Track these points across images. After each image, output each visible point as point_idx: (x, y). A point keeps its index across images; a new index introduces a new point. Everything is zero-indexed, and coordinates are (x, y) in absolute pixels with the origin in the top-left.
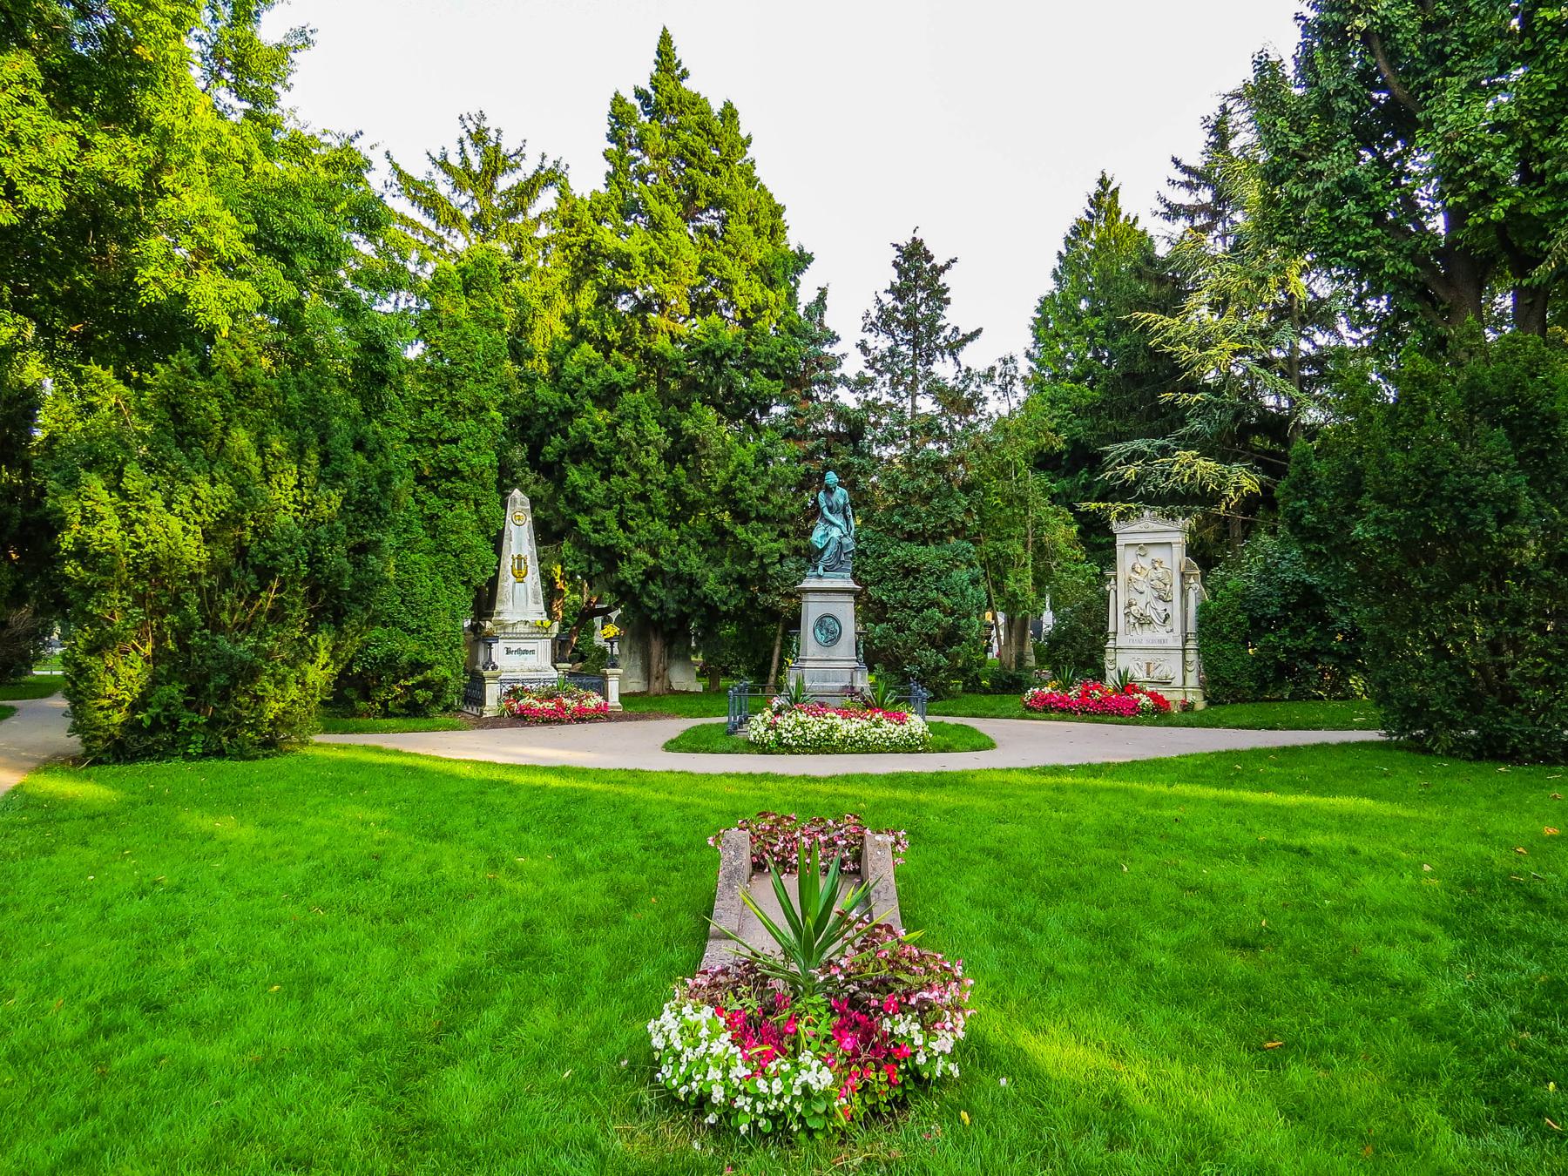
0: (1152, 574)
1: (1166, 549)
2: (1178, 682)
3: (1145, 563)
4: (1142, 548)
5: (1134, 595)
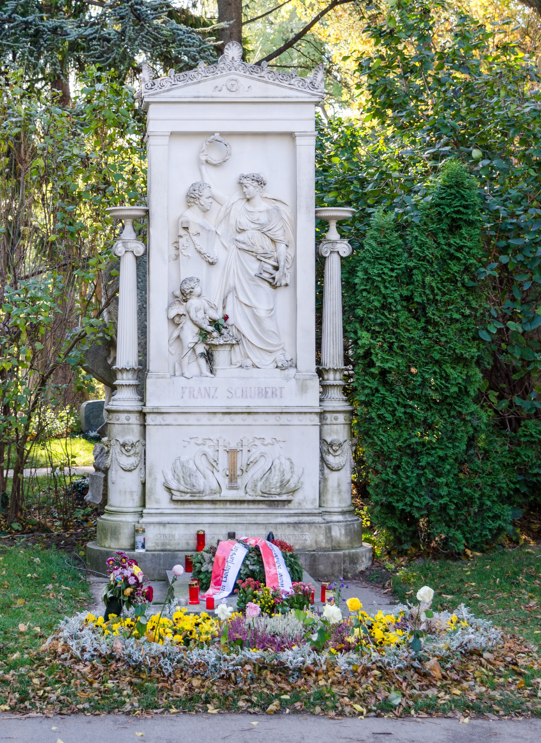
0: (240, 214)
1: (278, 149)
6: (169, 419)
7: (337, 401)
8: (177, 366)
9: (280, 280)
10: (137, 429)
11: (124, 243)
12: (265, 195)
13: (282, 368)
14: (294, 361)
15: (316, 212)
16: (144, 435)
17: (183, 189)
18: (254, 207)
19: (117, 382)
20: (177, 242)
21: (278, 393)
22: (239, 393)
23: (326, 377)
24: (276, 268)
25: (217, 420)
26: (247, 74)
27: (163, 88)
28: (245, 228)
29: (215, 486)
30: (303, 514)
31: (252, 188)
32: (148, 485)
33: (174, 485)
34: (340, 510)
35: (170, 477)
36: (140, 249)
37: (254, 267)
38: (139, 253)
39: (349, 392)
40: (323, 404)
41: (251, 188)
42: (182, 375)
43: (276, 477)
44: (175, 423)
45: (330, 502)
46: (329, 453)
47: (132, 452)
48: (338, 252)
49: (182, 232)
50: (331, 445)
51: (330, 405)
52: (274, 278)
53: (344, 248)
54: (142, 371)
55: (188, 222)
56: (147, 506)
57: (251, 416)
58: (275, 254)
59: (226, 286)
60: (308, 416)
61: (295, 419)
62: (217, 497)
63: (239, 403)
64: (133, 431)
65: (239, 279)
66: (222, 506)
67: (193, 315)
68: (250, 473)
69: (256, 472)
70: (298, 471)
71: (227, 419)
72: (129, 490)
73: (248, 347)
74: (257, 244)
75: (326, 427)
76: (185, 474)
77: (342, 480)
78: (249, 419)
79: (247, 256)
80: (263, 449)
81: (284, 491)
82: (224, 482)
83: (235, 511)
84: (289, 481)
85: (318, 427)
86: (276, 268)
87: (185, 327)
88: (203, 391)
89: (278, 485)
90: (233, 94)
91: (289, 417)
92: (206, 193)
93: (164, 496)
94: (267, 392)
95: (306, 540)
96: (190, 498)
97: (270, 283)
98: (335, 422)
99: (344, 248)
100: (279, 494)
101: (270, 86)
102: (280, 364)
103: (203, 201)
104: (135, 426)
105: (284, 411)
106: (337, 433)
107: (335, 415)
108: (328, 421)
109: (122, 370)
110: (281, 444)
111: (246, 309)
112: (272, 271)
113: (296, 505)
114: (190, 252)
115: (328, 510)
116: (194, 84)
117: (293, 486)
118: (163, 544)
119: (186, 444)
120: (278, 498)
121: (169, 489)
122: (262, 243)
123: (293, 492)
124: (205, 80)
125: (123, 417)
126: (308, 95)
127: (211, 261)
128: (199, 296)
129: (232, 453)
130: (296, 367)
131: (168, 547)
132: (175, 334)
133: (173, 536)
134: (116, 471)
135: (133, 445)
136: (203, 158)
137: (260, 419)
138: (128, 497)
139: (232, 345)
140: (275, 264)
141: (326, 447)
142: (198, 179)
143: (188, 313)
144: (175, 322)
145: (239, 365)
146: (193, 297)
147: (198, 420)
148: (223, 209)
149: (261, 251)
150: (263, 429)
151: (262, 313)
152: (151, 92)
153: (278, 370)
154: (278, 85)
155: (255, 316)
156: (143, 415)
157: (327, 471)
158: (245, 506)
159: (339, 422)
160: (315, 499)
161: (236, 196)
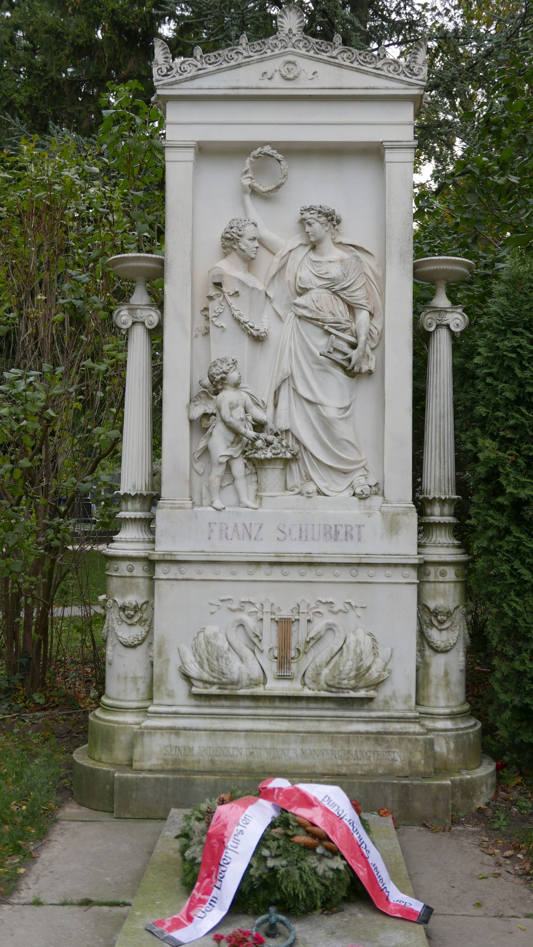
2: (402, 683)
3: (276, 226)
4: (264, 163)
5: (229, 346)
6: (190, 572)
7: (444, 548)
8: (204, 491)
9: (358, 362)
10: (143, 584)
11: (132, 310)
12: (339, 239)
13: (362, 497)
14: (380, 486)
15: (416, 267)
16: (151, 592)
17: (218, 231)
18: (322, 255)
20: (206, 309)
21: (355, 533)
22: (295, 533)
23: (429, 511)
24: (354, 346)
25: (261, 574)
26: (312, 53)
27: (185, 75)
28: (308, 286)
29: (256, 673)
31: (318, 227)
32: (156, 670)
33: (194, 670)
34: (447, 711)
36: (152, 317)
37: (319, 343)
38: (151, 323)
39: (462, 533)
40: (422, 550)
41: (317, 225)
42: (211, 504)
43: (350, 663)
44: (197, 577)
45: (433, 699)
46: (433, 625)
47: (136, 619)
48: (448, 326)
49: (213, 292)
50: (435, 613)
51: (435, 554)
52: (349, 360)
53: (457, 320)
54: (152, 499)
55: (221, 276)
56: (155, 701)
58: (354, 327)
59: (279, 372)
60: (400, 570)
61: (380, 575)
62: (259, 691)
63: (295, 549)
64: (138, 587)
65: (298, 361)
66: (267, 704)
67: (225, 413)
68: (311, 655)
69: (320, 654)
70: (384, 652)
71: (277, 573)
72: (131, 675)
73: (311, 464)
74: (325, 309)
75: (428, 586)
76: (210, 656)
77: (450, 665)
78: (311, 574)
79: (309, 327)
80: (331, 619)
81: (361, 684)
82: (271, 668)
83: (287, 712)
84: (369, 668)
85: (415, 587)
86: (354, 346)
87: (215, 432)
88: (240, 528)
89: (353, 674)
90: (290, 85)
91: (371, 571)
92: (249, 231)
93: (180, 688)
94: (337, 533)
95: (394, 760)
97: (344, 368)
98: (441, 579)
99: (457, 320)
101: (345, 72)
102: (358, 491)
103: (245, 244)
104: (141, 581)
105: (363, 561)
106: (444, 595)
107: (442, 568)
108: (431, 578)
109: (127, 497)
110: (359, 612)
111: (308, 407)
112: (345, 348)
113: (381, 704)
114: (225, 321)
115: (430, 710)
117: (375, 675)
119: (213, 609)
120: (352, 694)
121: (187, 678)
123: (377, 685)
124: (248, 64)
125: (123, 566)
126: (403, 86)
127: (255, 333)
128: (236, 386)
130: (383, 495)
131: (182, 766)
132: (202, 445)
133: (191, 749)
134: (114, 646)
135: (136, 609)
136: (247, 182)
137: (328, 574)
138: (130, 685)
139: (287, 462)
140: (352, 339)
142: (239, 214)
143: (219, 410)
144: (200, 425)
145: (297, 490)
146: (228, 387)
147: (233, 574)
148: (276, 260)
149: (330, 318)
151: (331, 413)
152: (167, 80)
153: (355, 499)
154: (358, 70)
157: (428, 652)
158: (304, 704)
159: (447, 579)
160: (410, 696)
161: (296, 240)
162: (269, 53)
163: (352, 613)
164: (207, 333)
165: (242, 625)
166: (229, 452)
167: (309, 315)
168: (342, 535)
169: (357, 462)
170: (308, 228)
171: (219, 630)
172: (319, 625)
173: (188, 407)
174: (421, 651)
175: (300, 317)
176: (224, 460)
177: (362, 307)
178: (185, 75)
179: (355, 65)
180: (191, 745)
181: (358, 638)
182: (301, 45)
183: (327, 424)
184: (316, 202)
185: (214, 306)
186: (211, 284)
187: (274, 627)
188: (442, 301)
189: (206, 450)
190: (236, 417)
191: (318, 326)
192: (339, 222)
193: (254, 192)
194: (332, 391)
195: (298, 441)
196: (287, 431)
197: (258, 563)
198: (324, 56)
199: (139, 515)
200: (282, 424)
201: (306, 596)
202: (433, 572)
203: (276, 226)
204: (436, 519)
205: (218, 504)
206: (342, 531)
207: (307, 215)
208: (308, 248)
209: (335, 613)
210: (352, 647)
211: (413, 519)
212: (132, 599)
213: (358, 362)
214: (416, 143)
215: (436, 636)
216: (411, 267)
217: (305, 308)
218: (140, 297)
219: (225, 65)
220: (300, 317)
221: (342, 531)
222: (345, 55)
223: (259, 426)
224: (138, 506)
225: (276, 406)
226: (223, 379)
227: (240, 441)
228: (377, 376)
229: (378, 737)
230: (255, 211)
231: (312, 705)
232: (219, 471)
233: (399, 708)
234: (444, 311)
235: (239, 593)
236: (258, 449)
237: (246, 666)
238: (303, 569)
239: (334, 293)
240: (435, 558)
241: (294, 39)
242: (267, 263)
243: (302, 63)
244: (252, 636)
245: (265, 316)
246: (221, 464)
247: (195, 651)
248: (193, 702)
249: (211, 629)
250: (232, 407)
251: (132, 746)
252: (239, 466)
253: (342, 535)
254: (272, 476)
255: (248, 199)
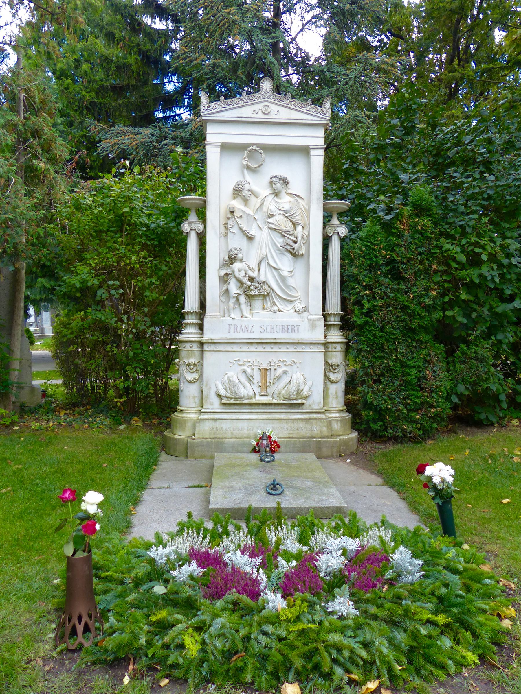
0: (271, 204)
2: (317, 397)
5: (237, 242)
6: (220, 348)
7: (336, 336)
9: (298, 250)
10: (197, 354)
11: (190, 224)
12: (289, 191)
13: (299, 313)
15: (324, 205)
19: (186, 321)
20: (226, 224)
21: (296, 329)
22: (269, 329)
23: (328, 319)
24: (295, 242)
25: (252, 348)
26: (276, 102)
27: (216, 110)
28: (274, 214)
29: (251, 393)
30: (312, 413)
33: (222, 392)
34: (337, 409)
35: (220, 387)
36: (200, 227)
37: (279, 241)
41: (278, 185)
42: (229, 316)
47: (194, 370)
49: (229, 216)
50: (332, 365)
52: (294, 249)
53: (343, 231)
55: (233, 208)
56: (204, 407)
57: (277, 346)
59: (262, 255)
61: (307, 349)
62: (253, 401)
65: (270, 249)
66: (256, 407)
67: (236, 273)
68: (276, 385)
69: (281, 384)
70: (309, 383)
71: (260, 348)
76: (231, 386)
77: (338, 389)
78: (276, 348)
79: (275, 233)
80: (285, 368)
81: (299, 397)
82: (258, 390)
86: (295, 242)
87: (231, 282)
89: (295, 393)
90: (266, 117)
91: (304, 346)
93: (216, 401)
94: (288, 329)
96: (234, 402)
97: (291, 253)
99: (343, 231)
100: (296, 399)
102: (297, 310)
103: (245, 193)
106: (335, 357)
109: (189, 313)
110: (298, 365)
111: (274, 272)
112: (292, 244)
114: (235, 230)
116: (238, 107)
118: (214, 434)
120: (295, 402)
121: (219, 396)
122: (286, 225)
124: (246, 105)
125: (188, 346)
128: (241, 260)
129: (264, 372)
131: (218, 436)
133: (222, 428)
135: (195, 365)
136: (245, 163)
137: (284, 349)
138: (192, 400)
139: (264, 296)
140: (295, 239)
141: (329, 367)
142: (241, 178)
143: (233, 272)
144: (224, 279)
148: (259, 201)
149: (285, 229)
150: (285, 355)
151: (285, 273)
152: (207, 112)
154: (298, 111)
155: (281, 276)
156: (202, 344)
157: (328, 383)
158: (273, 407)
161: (268, 191)
162: (256, 101)
163: (295, 366)
164: (226, 235)
165: (244, 372)
166: (238, 292)
167: (275, 227)
168: (290, 330)
169: (297, 297)
170: (274, 186)
171: (234, 374)
172: (280, 371)
173: (219, 270)
174: (325, 383)
175: (271, 229)
176: (236, 295)
177: (299, 224)
178: (216, 110)
179: (297, 108)
180: (222, 426)
181: (297, 377)
182: (272, 97)
183: (283, 279)
184: (278, 174)
185: (230, 222)
186: (228, 212)
187: (259, 372)
188: (335, 221)
189: (227, 291)
190: (241, 275)
191: (279, 233)
192: (288, 183)
193: (248, 167)
194: (285, 263)
195: (269, 287)
196: (264, 282)
197: (252, 343)
198: (282, 103)
199: (195, 321)
200: (262, 278)
201: (274, 358)
202: (331, 347)
203: (259, 184)
204: (332, 323)
205: (233, 316)
206: (290, 328)
207: (274, 180)
208: (273, 195)
209: (287, 366)
210: (295, 381)
211: (322, 323)
212: (193, 361)
213: (298, 250)
214: (325, 146)
215: (333, 376)
216: (321, 205)
217: (273, 224)
218: (193, 217)
219: (235, 106)
220: (271, 229)
221: (290, 328)
222: (292, 103)
223: (251, 279)
224: (194, 317)
225: (259, 270)
226: (235, 257)
227: (243, 286)
228: (305, 257)
229: (307, 420)
230: (249, 177)
231: (276, 407)
232: (232, 301)
233: (316, 407)
234: (336, 226)
235: (244, 357)
236: (251, 290)
237: (246, 390)
238: (272, 346)
239: (287, 217)
240: (332, 341)
241: (268, 94)
242: (255, 202)
243: (271, 106)
244: (249, 376)
245: (253, 227)
246: (234, 297)
247: (223, 384)
248: (222, 407)
249: (230, 374)
250: (239, 271)
251: (194, 427)
252: (242, 299)
253: (290, 330)
254: (258, 303)
255: (246, 172)
